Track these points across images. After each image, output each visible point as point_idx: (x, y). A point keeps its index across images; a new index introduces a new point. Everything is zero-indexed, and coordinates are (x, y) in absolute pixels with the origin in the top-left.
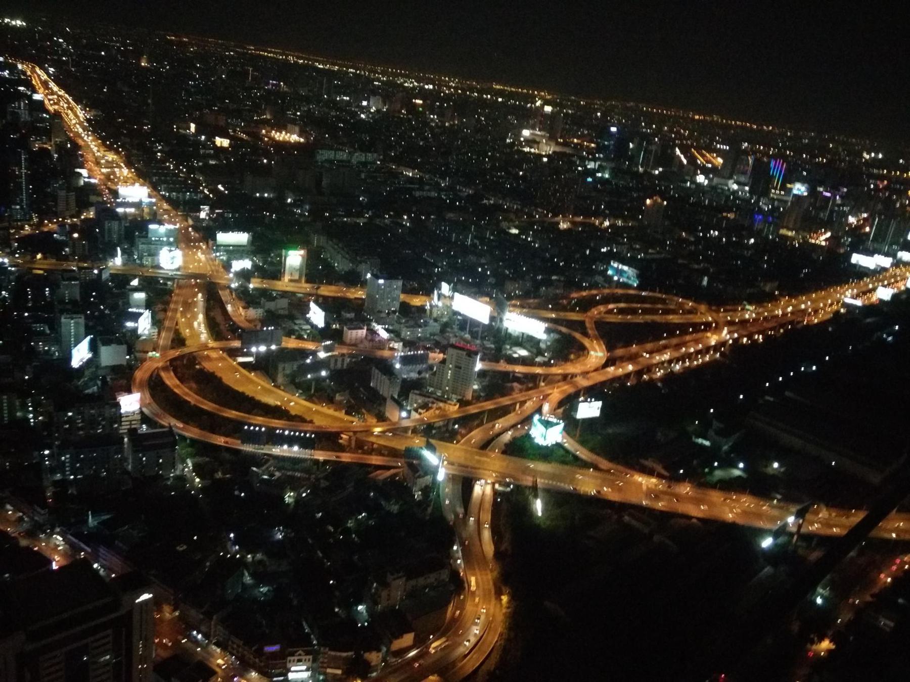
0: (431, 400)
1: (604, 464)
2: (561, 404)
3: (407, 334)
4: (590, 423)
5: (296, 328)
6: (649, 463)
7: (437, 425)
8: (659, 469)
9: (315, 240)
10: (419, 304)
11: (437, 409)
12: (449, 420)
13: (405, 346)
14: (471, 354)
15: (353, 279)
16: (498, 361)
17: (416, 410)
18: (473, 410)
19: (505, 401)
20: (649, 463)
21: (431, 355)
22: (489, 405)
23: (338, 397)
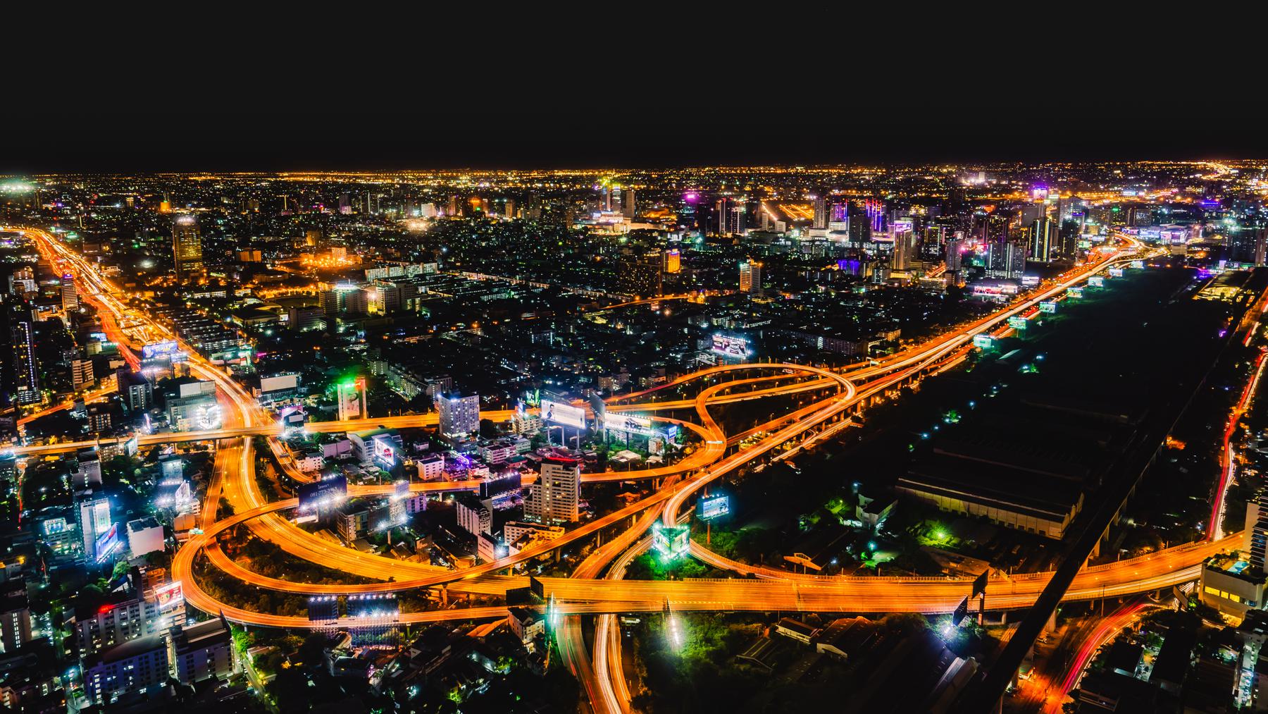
0: (530, 530)
1: (744, 569)
2: (684, 507)
3: (490, 456)
4: (721, 525)
5: (363, 471)
6: (795, 559)
7: (542, 558)
8: (808, 563)
9: (376, 368)
10: (502, 420)
11: (540, 539)
12: (555, 550)
13: (492, 471)
14: (569, 466)
15: (423, 404)
16: (603, 471)
17: (514, 545)
18: (581, 532)
19: (618, 516)
20: (795, 559)
21: (523, 476)
22: (600, 524)
23: (420, 546)
